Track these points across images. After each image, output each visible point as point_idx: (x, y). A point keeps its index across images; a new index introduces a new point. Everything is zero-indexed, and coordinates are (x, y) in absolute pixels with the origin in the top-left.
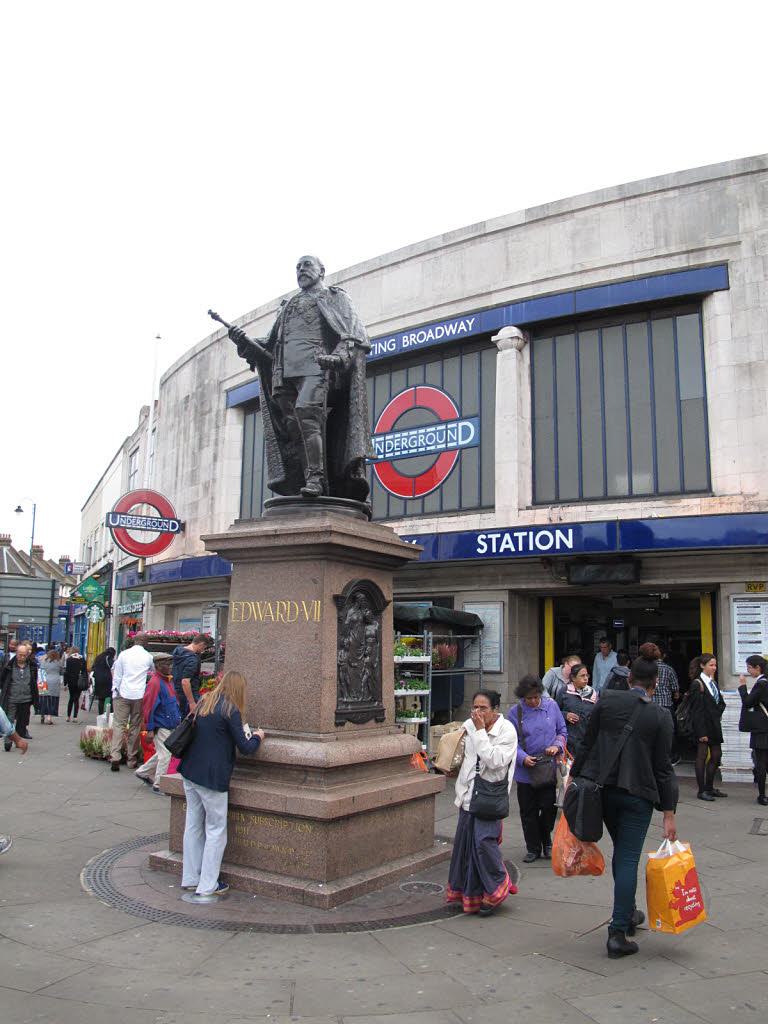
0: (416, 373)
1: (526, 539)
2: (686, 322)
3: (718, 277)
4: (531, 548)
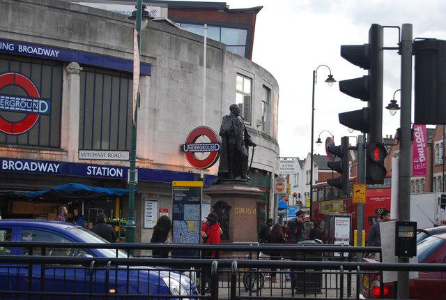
1: (106, 170)
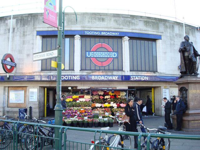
2: (154, 43)
3: (159, 37)
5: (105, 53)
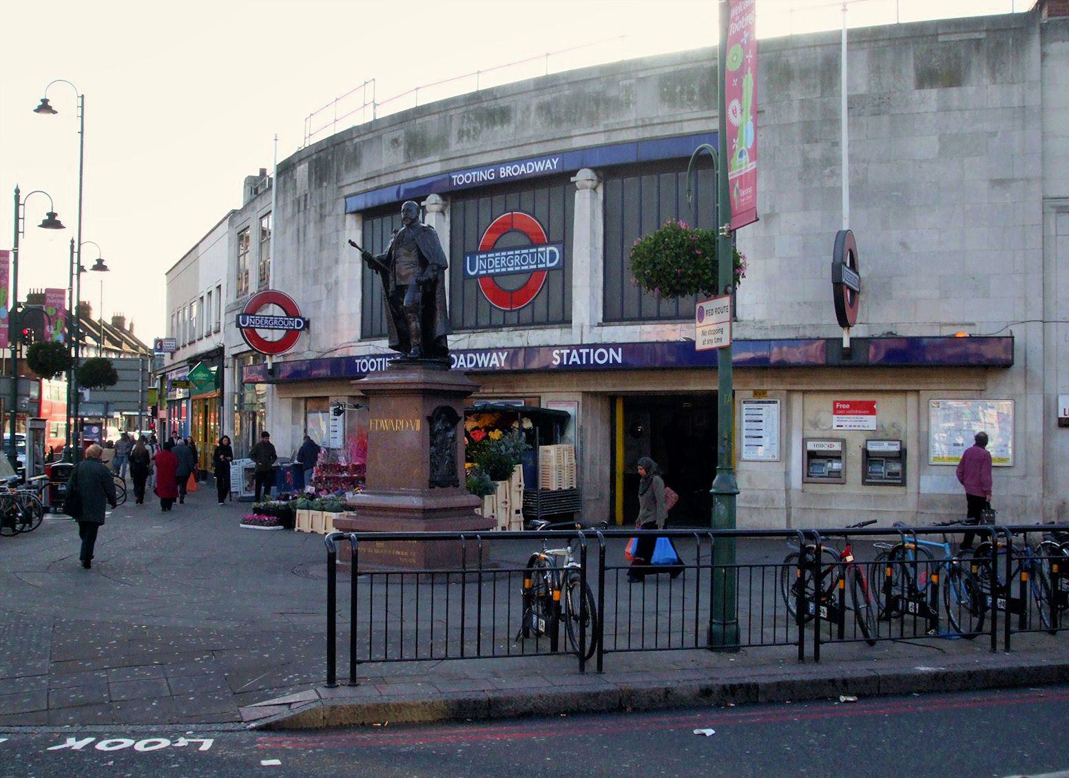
0: (513, 198)
1: (588, 354)
4: (592, 362)
5: (523, 251)
